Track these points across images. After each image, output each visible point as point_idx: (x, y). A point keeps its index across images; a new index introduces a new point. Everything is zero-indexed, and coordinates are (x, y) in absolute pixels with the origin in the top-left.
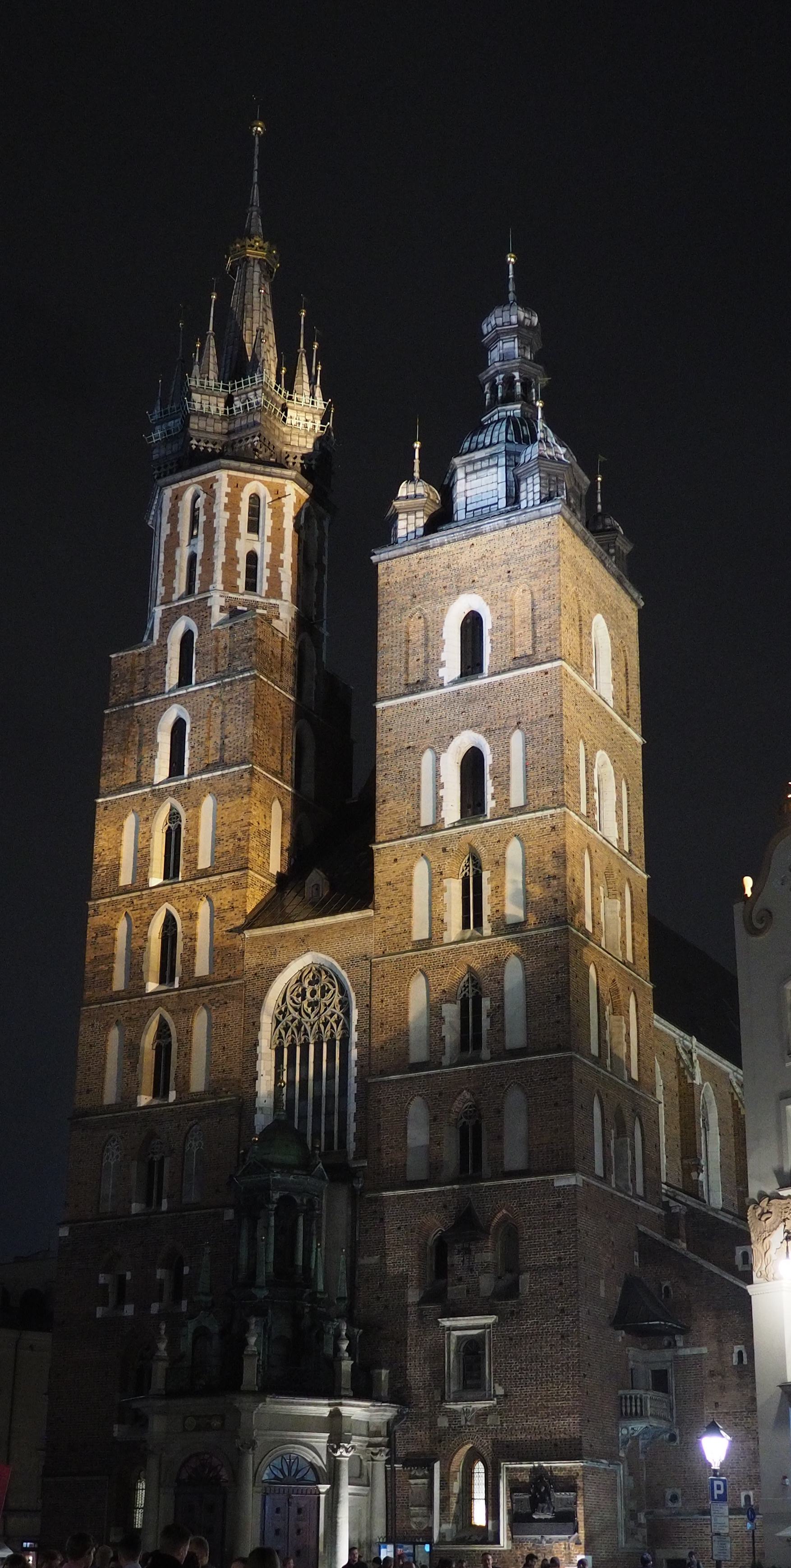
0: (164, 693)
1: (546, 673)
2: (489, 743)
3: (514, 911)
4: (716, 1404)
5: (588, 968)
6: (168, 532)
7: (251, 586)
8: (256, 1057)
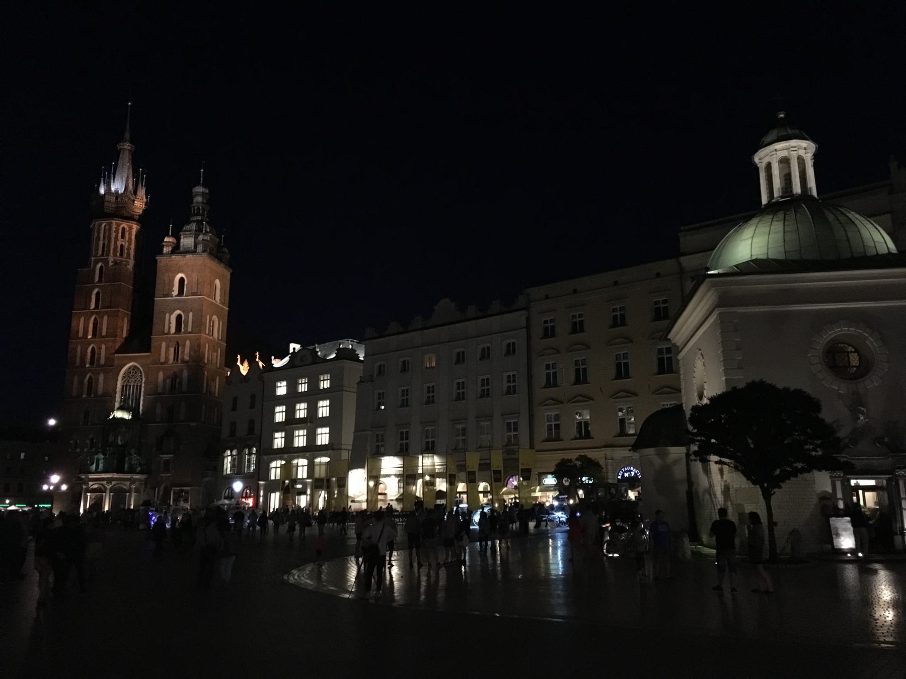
0: (94, 284)
3: (186, 358)
5: (204, 372)
7: (121, 255)
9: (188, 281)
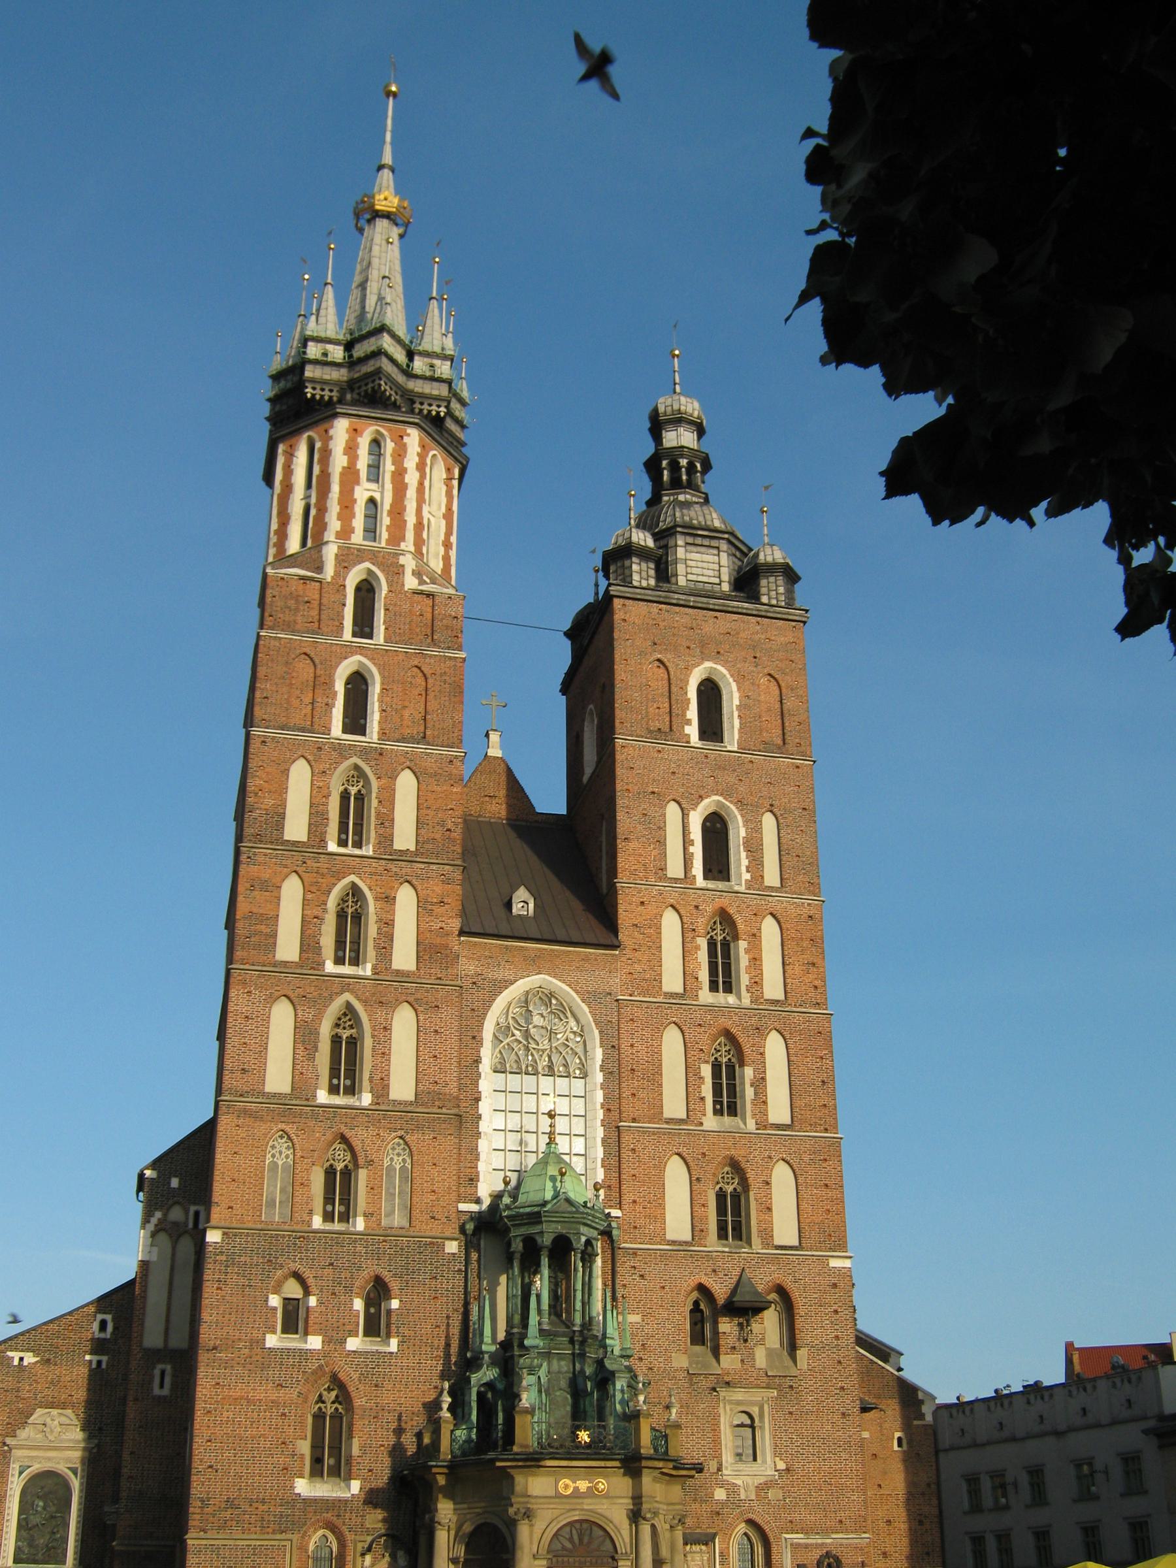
1: (798, 767)
2: (742, 815)
4: (880, 1486)
6: (345, 465)
8: (479, 1075)
9: (745, 697)
